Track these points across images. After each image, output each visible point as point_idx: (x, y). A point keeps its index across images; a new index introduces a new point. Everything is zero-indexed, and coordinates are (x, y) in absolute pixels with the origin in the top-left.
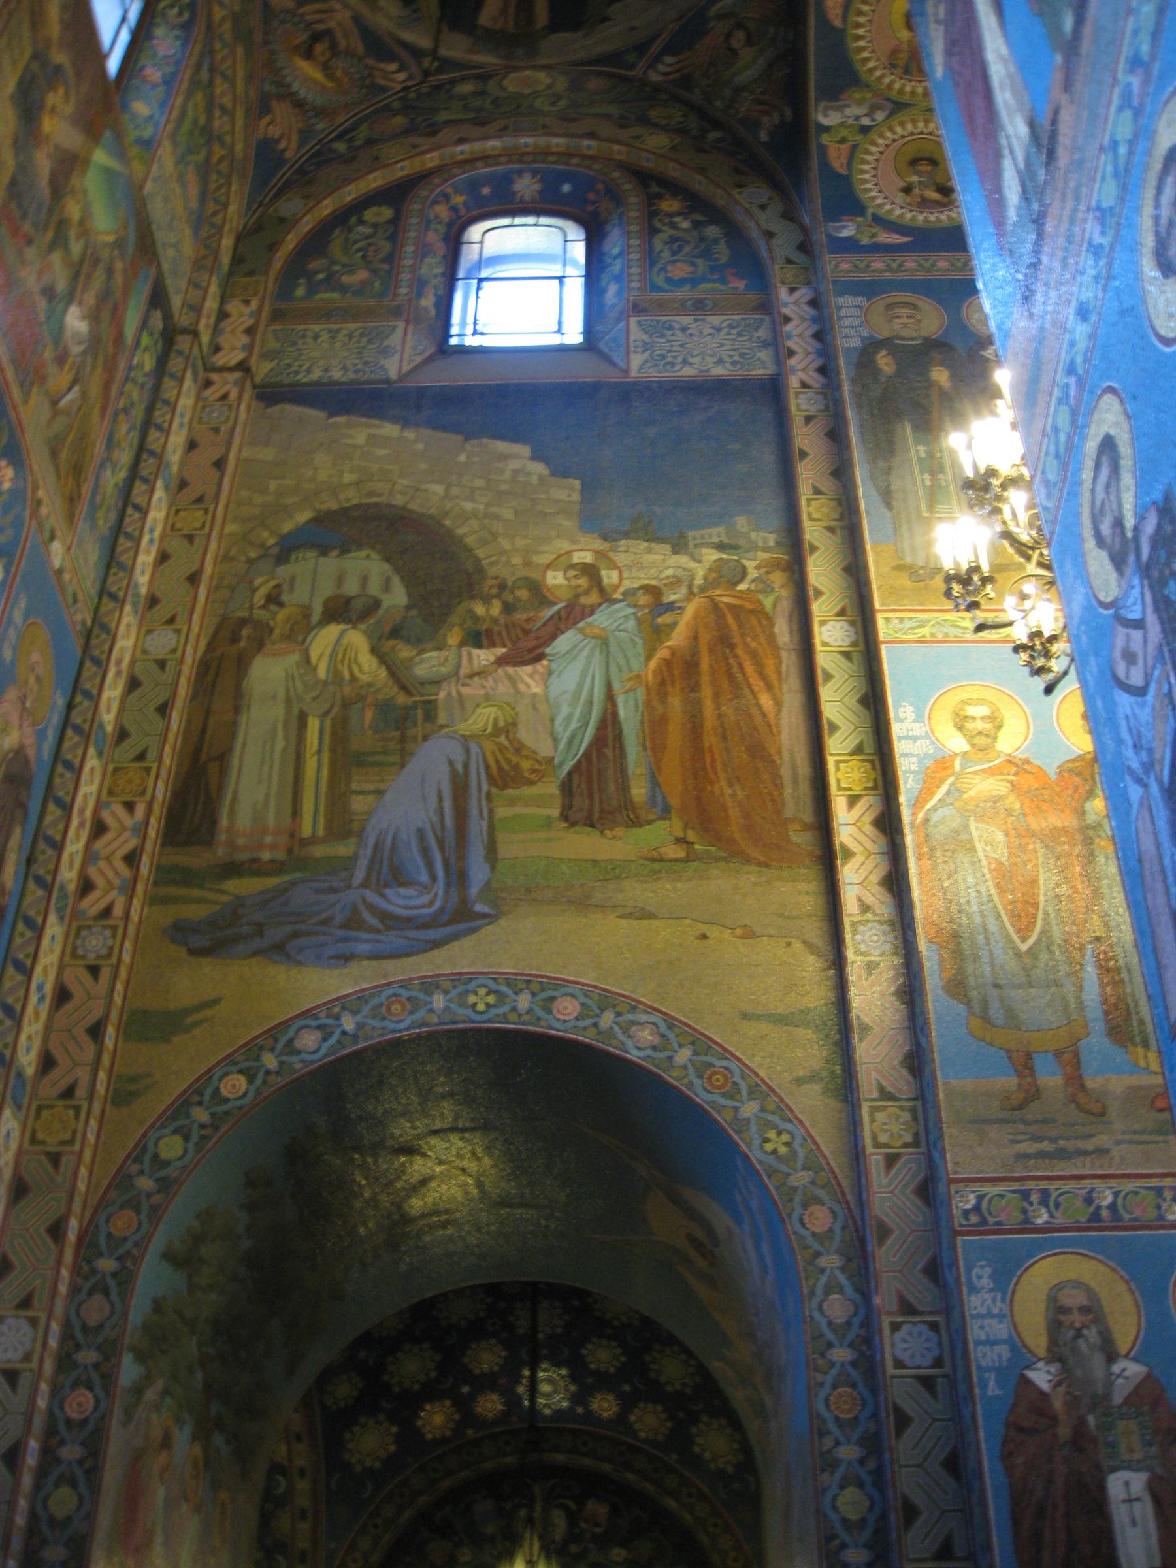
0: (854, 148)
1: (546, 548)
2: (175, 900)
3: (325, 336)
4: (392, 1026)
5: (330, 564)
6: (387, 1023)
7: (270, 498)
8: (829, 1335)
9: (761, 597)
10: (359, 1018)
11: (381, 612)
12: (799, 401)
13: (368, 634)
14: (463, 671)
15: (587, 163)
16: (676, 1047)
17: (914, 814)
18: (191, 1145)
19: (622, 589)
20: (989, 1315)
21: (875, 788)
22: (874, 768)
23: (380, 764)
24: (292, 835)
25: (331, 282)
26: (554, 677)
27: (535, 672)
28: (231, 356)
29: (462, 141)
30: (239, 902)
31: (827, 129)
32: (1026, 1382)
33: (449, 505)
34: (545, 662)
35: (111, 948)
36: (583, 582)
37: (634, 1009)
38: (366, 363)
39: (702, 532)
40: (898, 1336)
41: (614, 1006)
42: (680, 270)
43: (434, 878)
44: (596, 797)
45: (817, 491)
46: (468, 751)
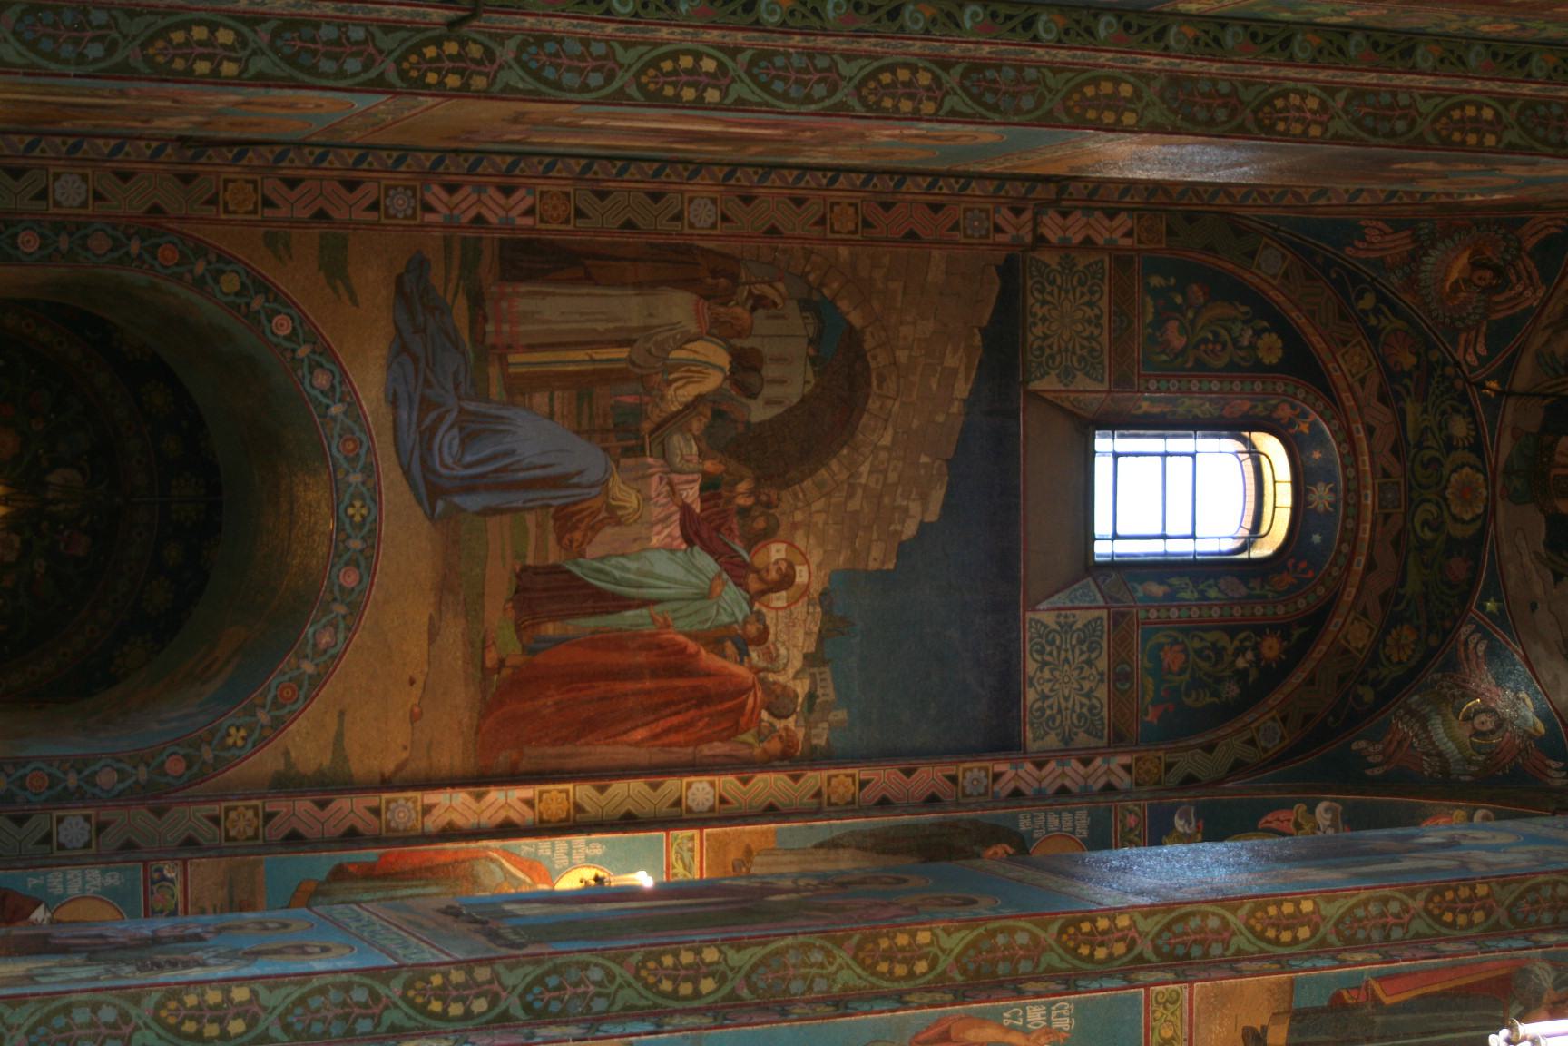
1: (812, 541)
6: (336, 440)
8: (86, 772)
9: (753, 731)
11: (744, 400)
12: (976, 771)
13: (717, 391)
14: (676, 478)
15: (1342, 560)
16: (316, 661)
17: (496, 850)
18: (231, 298)
19: (764, 610)
20: (85, 882)
21: (542, 821)
24: (509, 347)
26: (666, 554)
27: (674, 539)
28: (1052, 228)
29: (1370, 431)
31: (1311, 811)
32: (37, 905)
35: (395, 217)
36: (773, 575)
37: (348, 629)
38: (1052, 357)
39: (829, 681)
40: (81, 820)
42: (1172, 658)
45: (863, 784)
46: (592, 486)
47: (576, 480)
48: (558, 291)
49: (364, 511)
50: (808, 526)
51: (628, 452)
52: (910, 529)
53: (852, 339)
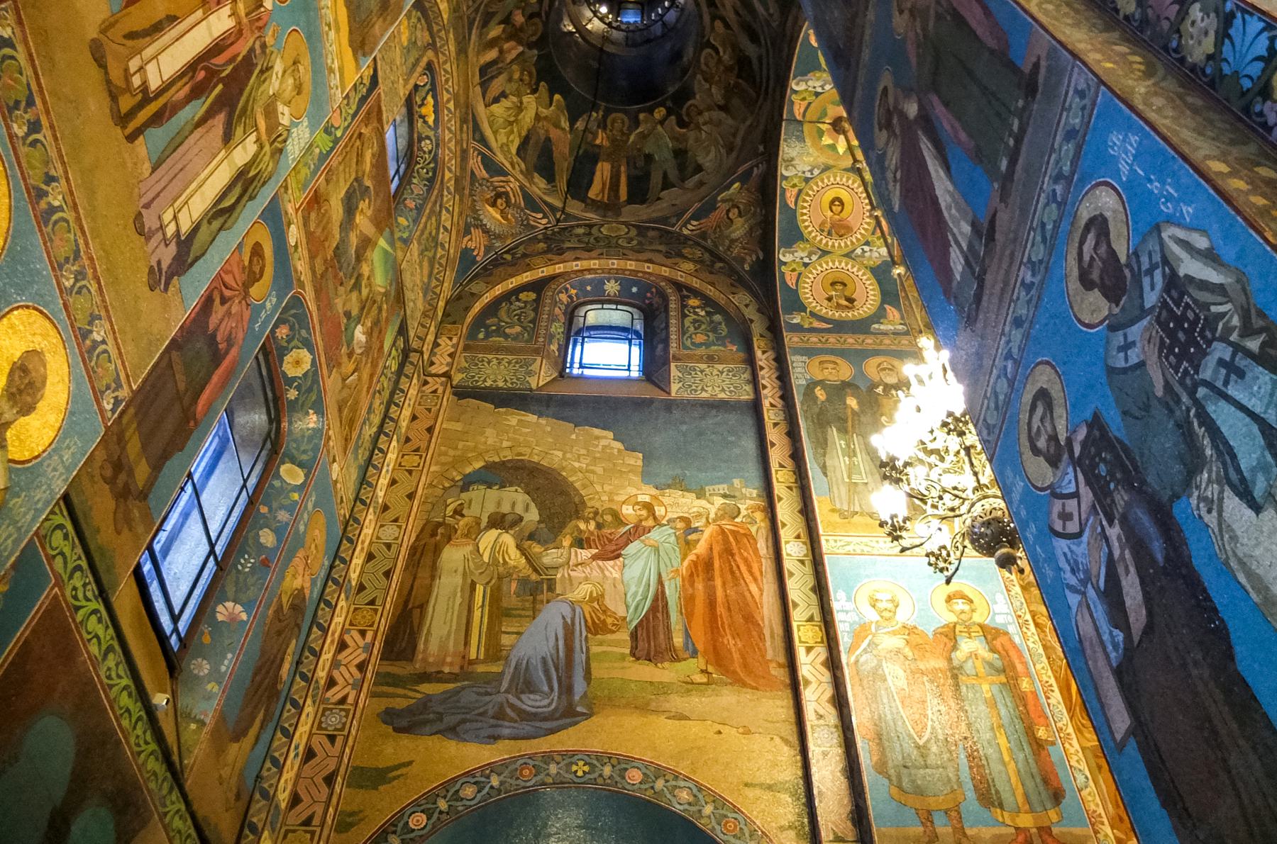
0: (800, 274)
2: (387, 695)
3: (495, 361)
4: (523, 784)
5: (493, 494)
6: (519, 782)
7: (459, 453)
9: (749, 526)
10: (502, 777)
19: (667, 518)
22: (821, 630)
23: (520, 616)
24: (464, 657)
25: (500, 332)
26: (626, 569)
28: (440, 368)
29: (577, 259)
30: (428, 698)
33: (564, 464)
34: (621, 559)
35: (344, 724)
36: (644, 513)
37: (676, 778)
41: (664, 776)
43: (551, 689)
44: (652, 644)
45: (781, 466)
46: (574, 610)
47: (569, 621)
48: (428, 625)
49: (581, 763)
50: (611, 494)
51: (551, 588)
52: (618, 445)
53: (489, 467)
